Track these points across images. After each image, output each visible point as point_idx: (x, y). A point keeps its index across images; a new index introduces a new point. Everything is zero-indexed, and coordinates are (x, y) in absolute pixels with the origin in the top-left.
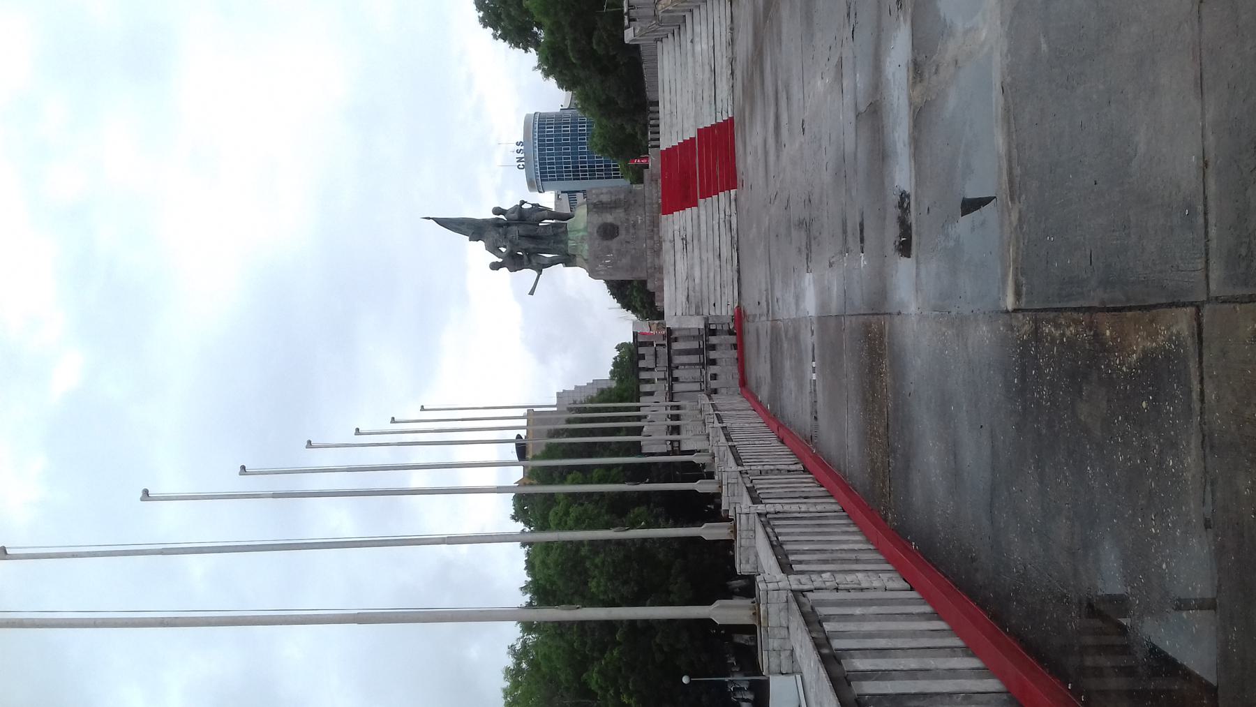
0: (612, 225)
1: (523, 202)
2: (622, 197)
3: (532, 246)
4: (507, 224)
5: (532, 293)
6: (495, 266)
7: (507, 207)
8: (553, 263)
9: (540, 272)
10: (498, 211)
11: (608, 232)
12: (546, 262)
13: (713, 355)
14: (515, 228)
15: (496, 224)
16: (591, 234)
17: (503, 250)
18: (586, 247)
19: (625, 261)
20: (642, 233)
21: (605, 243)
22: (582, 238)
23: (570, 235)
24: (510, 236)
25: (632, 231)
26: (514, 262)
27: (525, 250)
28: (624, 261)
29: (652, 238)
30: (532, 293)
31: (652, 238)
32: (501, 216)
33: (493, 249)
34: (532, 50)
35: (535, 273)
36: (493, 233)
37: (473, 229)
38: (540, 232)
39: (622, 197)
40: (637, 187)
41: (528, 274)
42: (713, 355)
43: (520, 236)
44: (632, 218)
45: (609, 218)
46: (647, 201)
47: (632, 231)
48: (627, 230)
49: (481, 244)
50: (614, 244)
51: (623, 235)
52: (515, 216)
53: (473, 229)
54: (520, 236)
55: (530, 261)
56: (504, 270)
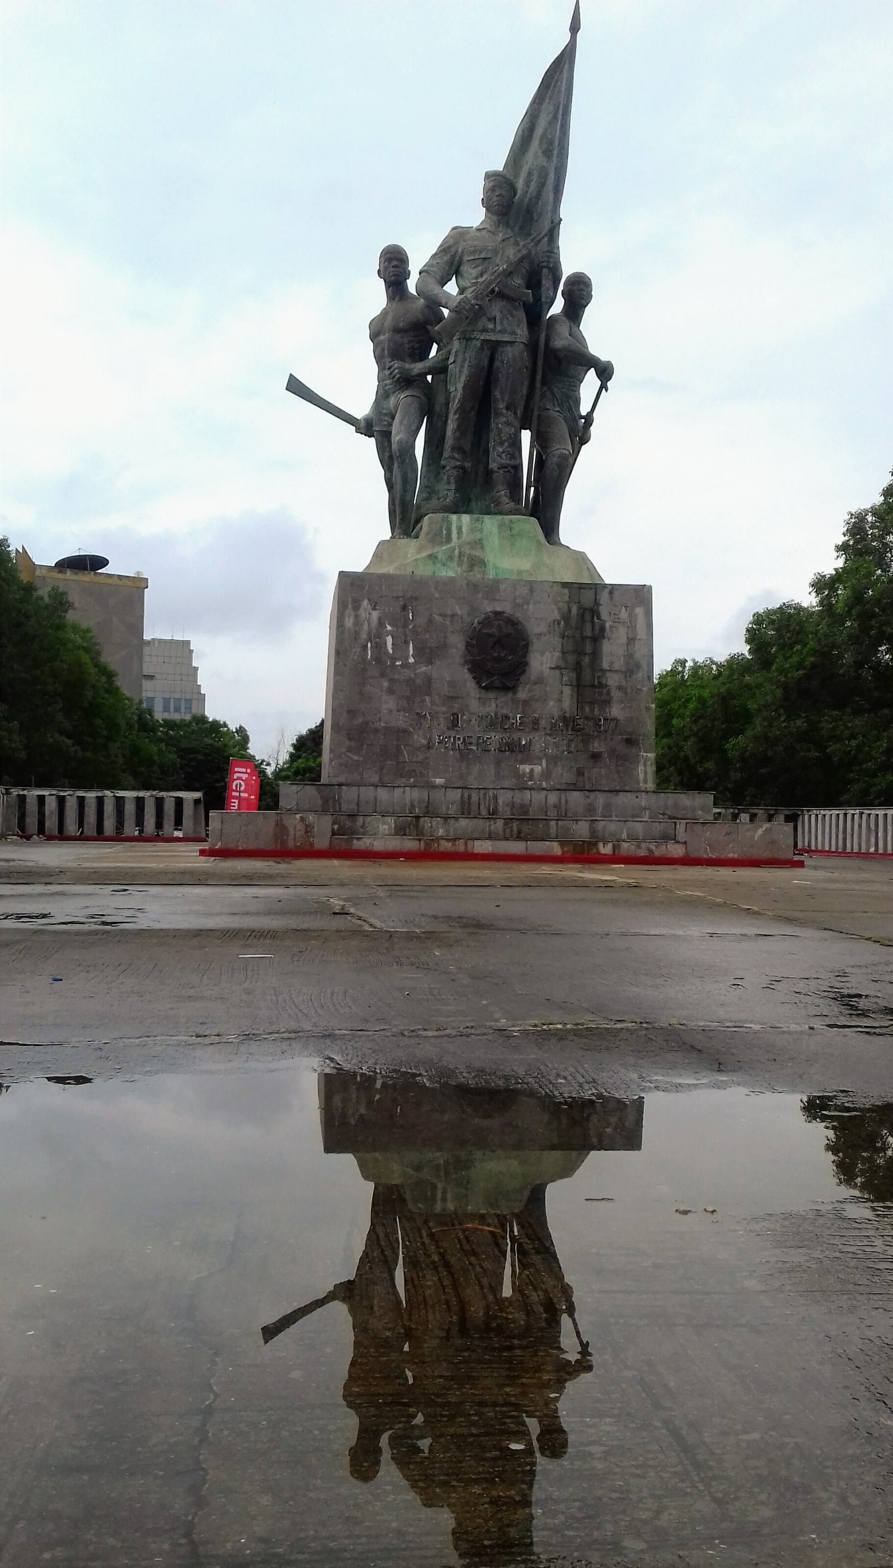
0: (519, 667)
1: (605, 372)
2: (616, 711)
3: (457, 388)
4: (534, 314)
5: (296, 387)
6: (393, 264)
8: (394, 460)
9: (366, 428)
10: (579, 293)
11: (497, 653)
12: (397, 436)
14: (522, 333)
15: (540, 269)
16: (492, 589)
17: (452, 288)
18: (449, 572)
19: (387, 709)
20: (483, 774)
21: (457, 643)
22: (475, 563)
23: (490, 523)
24: (497, 309)
25: (495, 738)
26: (406, 337)
27: (440, 370)
28: (389, 704)
29: (466, 810)
30: (296, 387)
31: (466, 810)
32: (558, 306)
33: (451, 258)
34: (840, 563)
35: (362, 408)
36: (511, 253)
37: (524, 198)
38: (501, 423)
39: (616, 711)
40: (645, 770)
41: (357, 381)
43: (493, 348)
44: (539, 742)
45: (543, 660)
46: (601, 799)
47: (495, 738)
48: (499, 722)
49: (474, 215)
50: (452, 671)
51: (478, 704)
52: (561, 340)
53: (524, 198)
55: (406, 382)
56: (375, 298)
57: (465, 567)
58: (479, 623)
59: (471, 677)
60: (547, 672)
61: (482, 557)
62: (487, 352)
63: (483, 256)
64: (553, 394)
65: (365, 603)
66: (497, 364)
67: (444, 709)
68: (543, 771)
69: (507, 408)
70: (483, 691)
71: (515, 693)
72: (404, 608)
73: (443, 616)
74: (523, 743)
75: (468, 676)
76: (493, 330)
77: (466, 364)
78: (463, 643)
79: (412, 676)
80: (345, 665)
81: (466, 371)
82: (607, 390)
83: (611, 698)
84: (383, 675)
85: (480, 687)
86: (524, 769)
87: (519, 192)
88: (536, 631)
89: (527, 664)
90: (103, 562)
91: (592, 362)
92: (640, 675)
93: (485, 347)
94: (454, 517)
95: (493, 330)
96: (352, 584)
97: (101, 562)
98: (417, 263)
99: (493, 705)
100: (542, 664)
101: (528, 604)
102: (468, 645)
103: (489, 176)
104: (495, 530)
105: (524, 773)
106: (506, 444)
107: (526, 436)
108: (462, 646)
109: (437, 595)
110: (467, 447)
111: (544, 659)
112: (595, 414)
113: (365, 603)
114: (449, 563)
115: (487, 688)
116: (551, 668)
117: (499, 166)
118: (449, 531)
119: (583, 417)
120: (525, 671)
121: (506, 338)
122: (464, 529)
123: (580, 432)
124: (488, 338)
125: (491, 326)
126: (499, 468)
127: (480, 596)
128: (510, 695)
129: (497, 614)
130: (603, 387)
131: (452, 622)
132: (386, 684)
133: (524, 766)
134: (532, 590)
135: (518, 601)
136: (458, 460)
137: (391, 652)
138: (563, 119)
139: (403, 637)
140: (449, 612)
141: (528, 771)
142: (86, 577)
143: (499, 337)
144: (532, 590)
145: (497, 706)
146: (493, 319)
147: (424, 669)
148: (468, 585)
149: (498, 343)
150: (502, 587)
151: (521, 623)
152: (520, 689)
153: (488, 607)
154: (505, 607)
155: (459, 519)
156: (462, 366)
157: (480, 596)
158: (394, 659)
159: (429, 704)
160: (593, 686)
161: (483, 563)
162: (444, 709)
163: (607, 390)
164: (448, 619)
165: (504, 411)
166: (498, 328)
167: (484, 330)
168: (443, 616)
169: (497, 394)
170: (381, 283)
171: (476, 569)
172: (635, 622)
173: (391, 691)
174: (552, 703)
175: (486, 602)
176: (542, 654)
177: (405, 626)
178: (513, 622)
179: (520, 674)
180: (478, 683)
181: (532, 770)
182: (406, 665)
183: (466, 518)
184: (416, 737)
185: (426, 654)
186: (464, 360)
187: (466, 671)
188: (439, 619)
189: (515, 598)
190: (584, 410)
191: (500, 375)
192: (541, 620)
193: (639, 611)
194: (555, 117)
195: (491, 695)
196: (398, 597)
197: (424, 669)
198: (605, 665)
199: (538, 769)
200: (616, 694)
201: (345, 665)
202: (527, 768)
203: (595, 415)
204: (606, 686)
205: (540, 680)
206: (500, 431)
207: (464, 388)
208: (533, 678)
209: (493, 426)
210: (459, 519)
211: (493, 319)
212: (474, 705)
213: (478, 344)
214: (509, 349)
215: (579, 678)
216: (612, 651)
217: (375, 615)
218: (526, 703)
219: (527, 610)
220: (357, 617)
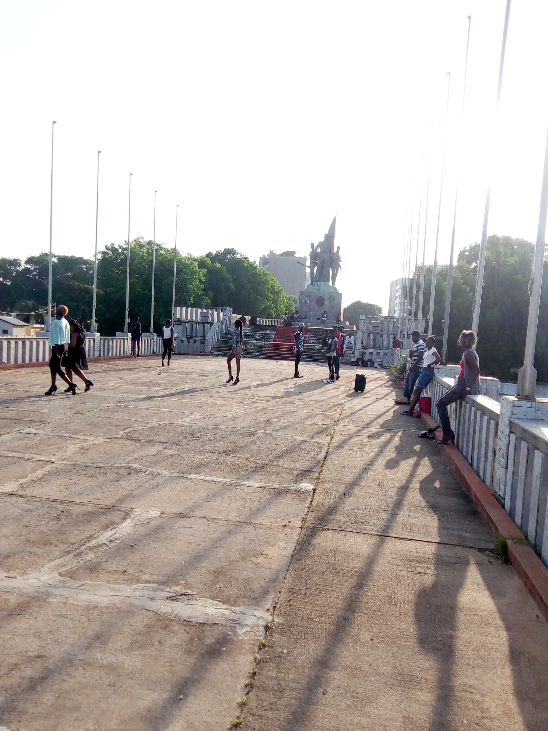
0: (323, 303)
6: (312, 245)
7: (341, 253)
10: (339, 248)
13: (192, 341)
15: (331, 247)
21: (315, 300)
33: (319, 246)
42: (192, 341)
49: (323, 239)
50: (314, 304)
56: (311, 250)
90: (295, 253)
97: (295, 253)
98: (315, 246)
103: (326, 235)
107: (331, 269)
117: (327, 233)
142: (289, 258)
192: (326, 297)
216: (336, 302)
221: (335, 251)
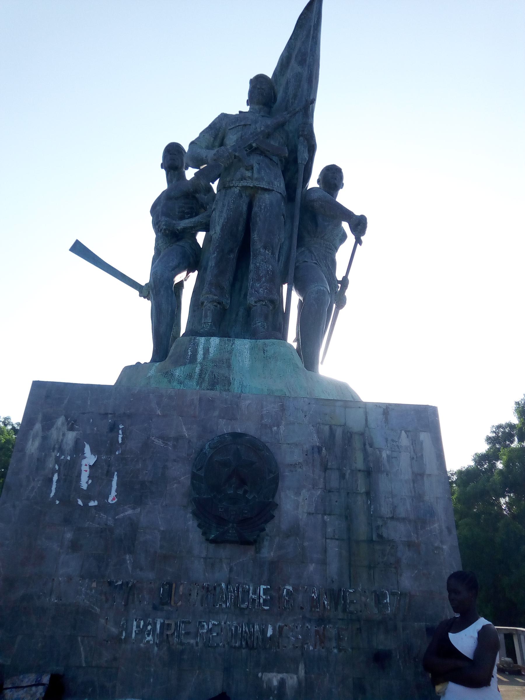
0: (266, 510)
1: (359, 225)
5: (79, 249)
6: (173, 158)
10: (333, 177)
14: (280, 185)
21: (180, 475)
24: (255, 160)
30: (79, 249)
35: (144, 278)
37: (284, 100)
41: (137, 249)
43: (252, 194)
50: (169, 517)
53: (284, 100)
54: (252, 194)
57: (205, 385)
58: (210, 447)
59: (196, 523)
60: (302, 517)
61: (227, 374)
62: (245, 200)
63: (242, 123)
64: (311, 252)
65: (60, 421)
66: (255, 209)
67: (151, 575)
68: (299, 682)
69: (265, 248)
70: (212, 546)
71: (258, 551)
72: (113, 428)
73: (164, 438)
74: (270, 633)
75: (192, 523)
76: (251, 178)
77: (225, 209)
78: (189, 476)
79: (111, 522)
80: (14, 506)
81: (224, 215)
82: (360, 244)
83: (398, 561)
84: (67, 521)
85: (207, 540)
86: (270, 681)
87: (280, 96)
88: (289, 459)
89: (276, 506)
91: (347, 215)
92: (436, 525)
93: (244, 195)
94: (202, 340)
95: (251, 178)
96: (47, 397)
99: (226, 568)
100: (297, 507)
101: (278, 426)
102: (194, 476)
104: (247, 354)
105: (270, 688)
106: (264, 279)
108: (186, 480)
109: (159, 412)
110: (226, 285)
111: (301, 499)
112: (348, 277)
113: (60, 421)
114: (187, 381)
115: (213, 541)
116: (309, 514)
118: (195, 353)
119: (339, 282)
120: (273, 517)
121: (264, 185)
122: (212, 350)
123: (337, 292)
124: (245, 184)
125: (248, 174)
126: (256, 302)
127: (216, 413)
128: (251, 551)
129: (236, 436)
130: (358, 241)
131: (174, 447)
132: (69, 536)
133: (270, 675)
134: (283, 408)
135: (265, 421)
136: (215, 295)
137: (84, 486)
138: (314, 33)
139: (106, 467)
140: (173, 434)
141: (275, 683)
143: (256, 184)
144: (283, 408)
145: (231, 570)
146: (251, 168)
147: (130, 512)
148: (200, 400)
149: (257, 189)
150: (244, 404)
151: (268, 450)
152: (266, 543)
153: (225, 427)
154: (247, 427)
155: (207, 341)
156: (222, 212)
157: (216, 413)
158: (87, 496)
159: (130, 568)
160: (370, 541)
161: (228, 382)
162: (151, 575)
163: (360, 244)
164: (170, 444)
165: (262, 250)
166: (256, 176)
167: (243, 178)
168: (164, 438)
169: (255, 236)
170: (163, 172)
171: (218, 387)
172: (422, 449)
173: (75, 546)
174: (312, 567)
175: (222, 422)
176: (298, 494)
177: (111, 452)
178: (255, 446)
179: (267, 521)
180: (204, 533)
181: (282, 682)
182: (103, 507)
183: (215, 341)
184: (102, 621)
185: (136, 491)
186: (224, 205)
187: (189, 515)
188: (159, 442)
189: (262, 417)
190: (339, 275)
191: (258, 219)
193: (424, 437)
194: (308, 36)
195: (224, 552)
196: (106, 414)
197: (130, 512)
198: (385, 510)
199: (292, 680)
200: (405, 555)
201: (14, 506)
202: (274, 678)
203: (349, 277)
204: (390, 542)
205: (295, 531)
206: (257, 268)
207: (222, 230)
208: (284, 526)
209: (252, 266)
210: (207, 341)
211: (251, 168)
212: (198, 569)
213: (237, 190)
214: (267, 196)
215: (349, 529)
217: (71, 436)
218: (274, 565)
219: (277, 433)
220: (45, 438)
221: (313, 183)
